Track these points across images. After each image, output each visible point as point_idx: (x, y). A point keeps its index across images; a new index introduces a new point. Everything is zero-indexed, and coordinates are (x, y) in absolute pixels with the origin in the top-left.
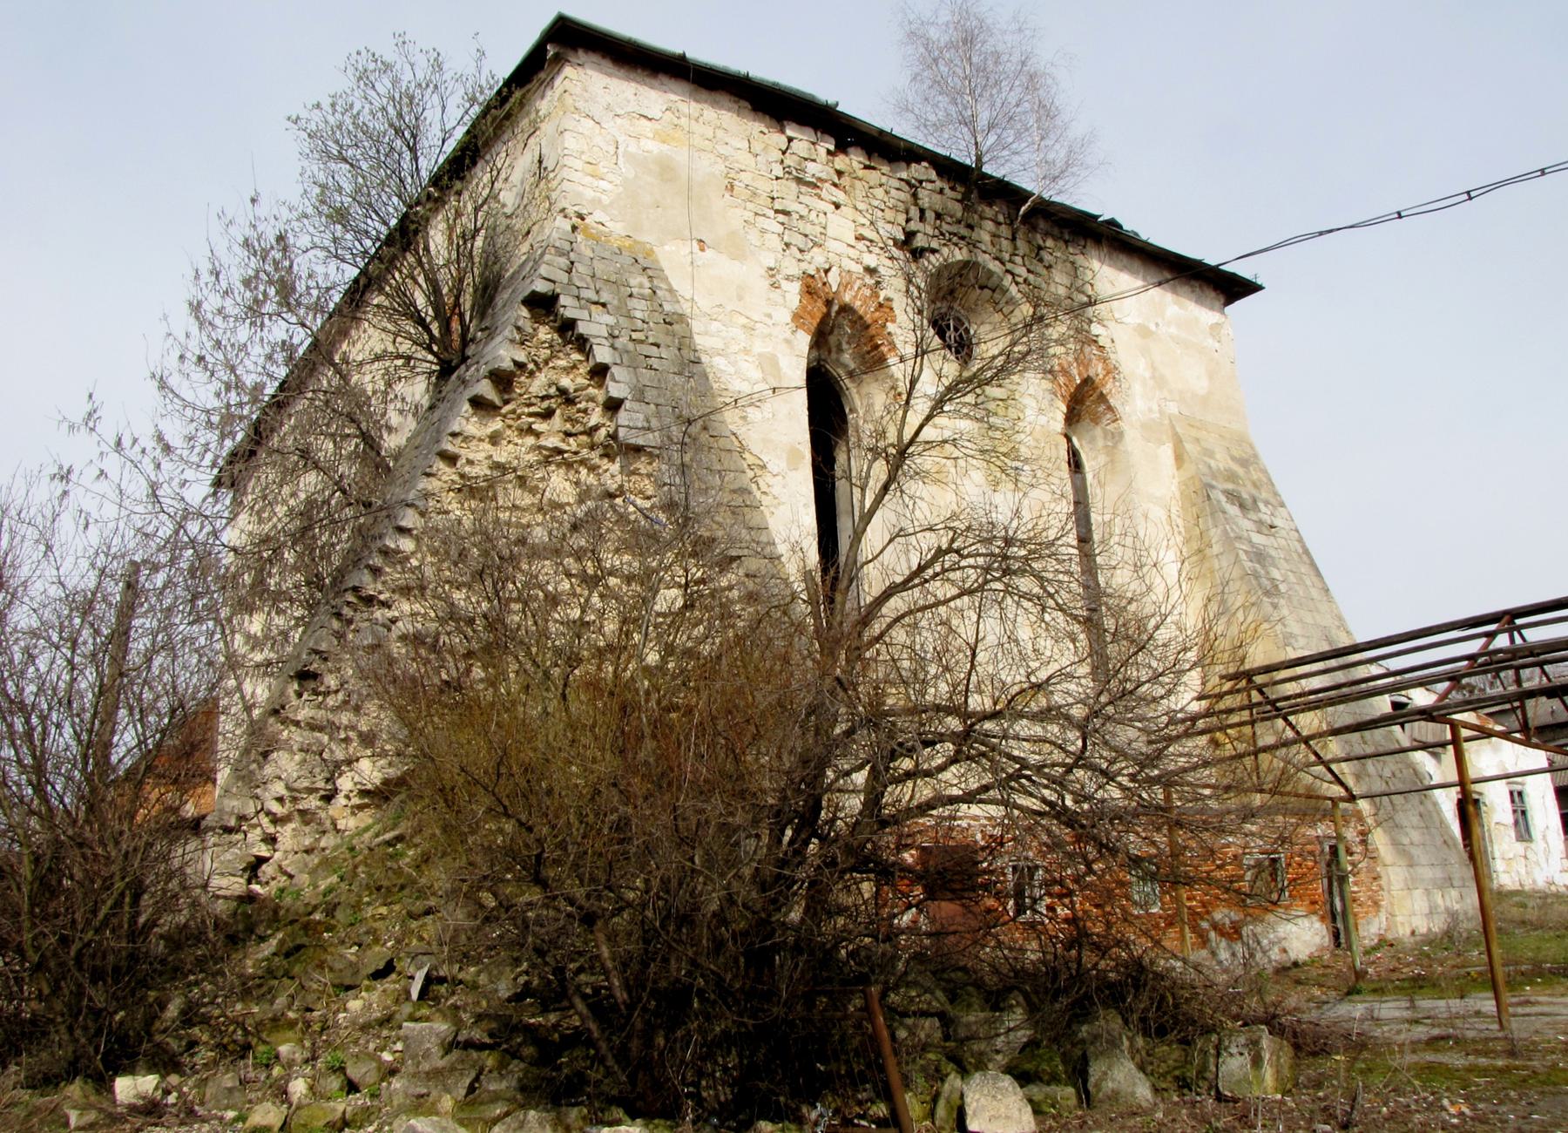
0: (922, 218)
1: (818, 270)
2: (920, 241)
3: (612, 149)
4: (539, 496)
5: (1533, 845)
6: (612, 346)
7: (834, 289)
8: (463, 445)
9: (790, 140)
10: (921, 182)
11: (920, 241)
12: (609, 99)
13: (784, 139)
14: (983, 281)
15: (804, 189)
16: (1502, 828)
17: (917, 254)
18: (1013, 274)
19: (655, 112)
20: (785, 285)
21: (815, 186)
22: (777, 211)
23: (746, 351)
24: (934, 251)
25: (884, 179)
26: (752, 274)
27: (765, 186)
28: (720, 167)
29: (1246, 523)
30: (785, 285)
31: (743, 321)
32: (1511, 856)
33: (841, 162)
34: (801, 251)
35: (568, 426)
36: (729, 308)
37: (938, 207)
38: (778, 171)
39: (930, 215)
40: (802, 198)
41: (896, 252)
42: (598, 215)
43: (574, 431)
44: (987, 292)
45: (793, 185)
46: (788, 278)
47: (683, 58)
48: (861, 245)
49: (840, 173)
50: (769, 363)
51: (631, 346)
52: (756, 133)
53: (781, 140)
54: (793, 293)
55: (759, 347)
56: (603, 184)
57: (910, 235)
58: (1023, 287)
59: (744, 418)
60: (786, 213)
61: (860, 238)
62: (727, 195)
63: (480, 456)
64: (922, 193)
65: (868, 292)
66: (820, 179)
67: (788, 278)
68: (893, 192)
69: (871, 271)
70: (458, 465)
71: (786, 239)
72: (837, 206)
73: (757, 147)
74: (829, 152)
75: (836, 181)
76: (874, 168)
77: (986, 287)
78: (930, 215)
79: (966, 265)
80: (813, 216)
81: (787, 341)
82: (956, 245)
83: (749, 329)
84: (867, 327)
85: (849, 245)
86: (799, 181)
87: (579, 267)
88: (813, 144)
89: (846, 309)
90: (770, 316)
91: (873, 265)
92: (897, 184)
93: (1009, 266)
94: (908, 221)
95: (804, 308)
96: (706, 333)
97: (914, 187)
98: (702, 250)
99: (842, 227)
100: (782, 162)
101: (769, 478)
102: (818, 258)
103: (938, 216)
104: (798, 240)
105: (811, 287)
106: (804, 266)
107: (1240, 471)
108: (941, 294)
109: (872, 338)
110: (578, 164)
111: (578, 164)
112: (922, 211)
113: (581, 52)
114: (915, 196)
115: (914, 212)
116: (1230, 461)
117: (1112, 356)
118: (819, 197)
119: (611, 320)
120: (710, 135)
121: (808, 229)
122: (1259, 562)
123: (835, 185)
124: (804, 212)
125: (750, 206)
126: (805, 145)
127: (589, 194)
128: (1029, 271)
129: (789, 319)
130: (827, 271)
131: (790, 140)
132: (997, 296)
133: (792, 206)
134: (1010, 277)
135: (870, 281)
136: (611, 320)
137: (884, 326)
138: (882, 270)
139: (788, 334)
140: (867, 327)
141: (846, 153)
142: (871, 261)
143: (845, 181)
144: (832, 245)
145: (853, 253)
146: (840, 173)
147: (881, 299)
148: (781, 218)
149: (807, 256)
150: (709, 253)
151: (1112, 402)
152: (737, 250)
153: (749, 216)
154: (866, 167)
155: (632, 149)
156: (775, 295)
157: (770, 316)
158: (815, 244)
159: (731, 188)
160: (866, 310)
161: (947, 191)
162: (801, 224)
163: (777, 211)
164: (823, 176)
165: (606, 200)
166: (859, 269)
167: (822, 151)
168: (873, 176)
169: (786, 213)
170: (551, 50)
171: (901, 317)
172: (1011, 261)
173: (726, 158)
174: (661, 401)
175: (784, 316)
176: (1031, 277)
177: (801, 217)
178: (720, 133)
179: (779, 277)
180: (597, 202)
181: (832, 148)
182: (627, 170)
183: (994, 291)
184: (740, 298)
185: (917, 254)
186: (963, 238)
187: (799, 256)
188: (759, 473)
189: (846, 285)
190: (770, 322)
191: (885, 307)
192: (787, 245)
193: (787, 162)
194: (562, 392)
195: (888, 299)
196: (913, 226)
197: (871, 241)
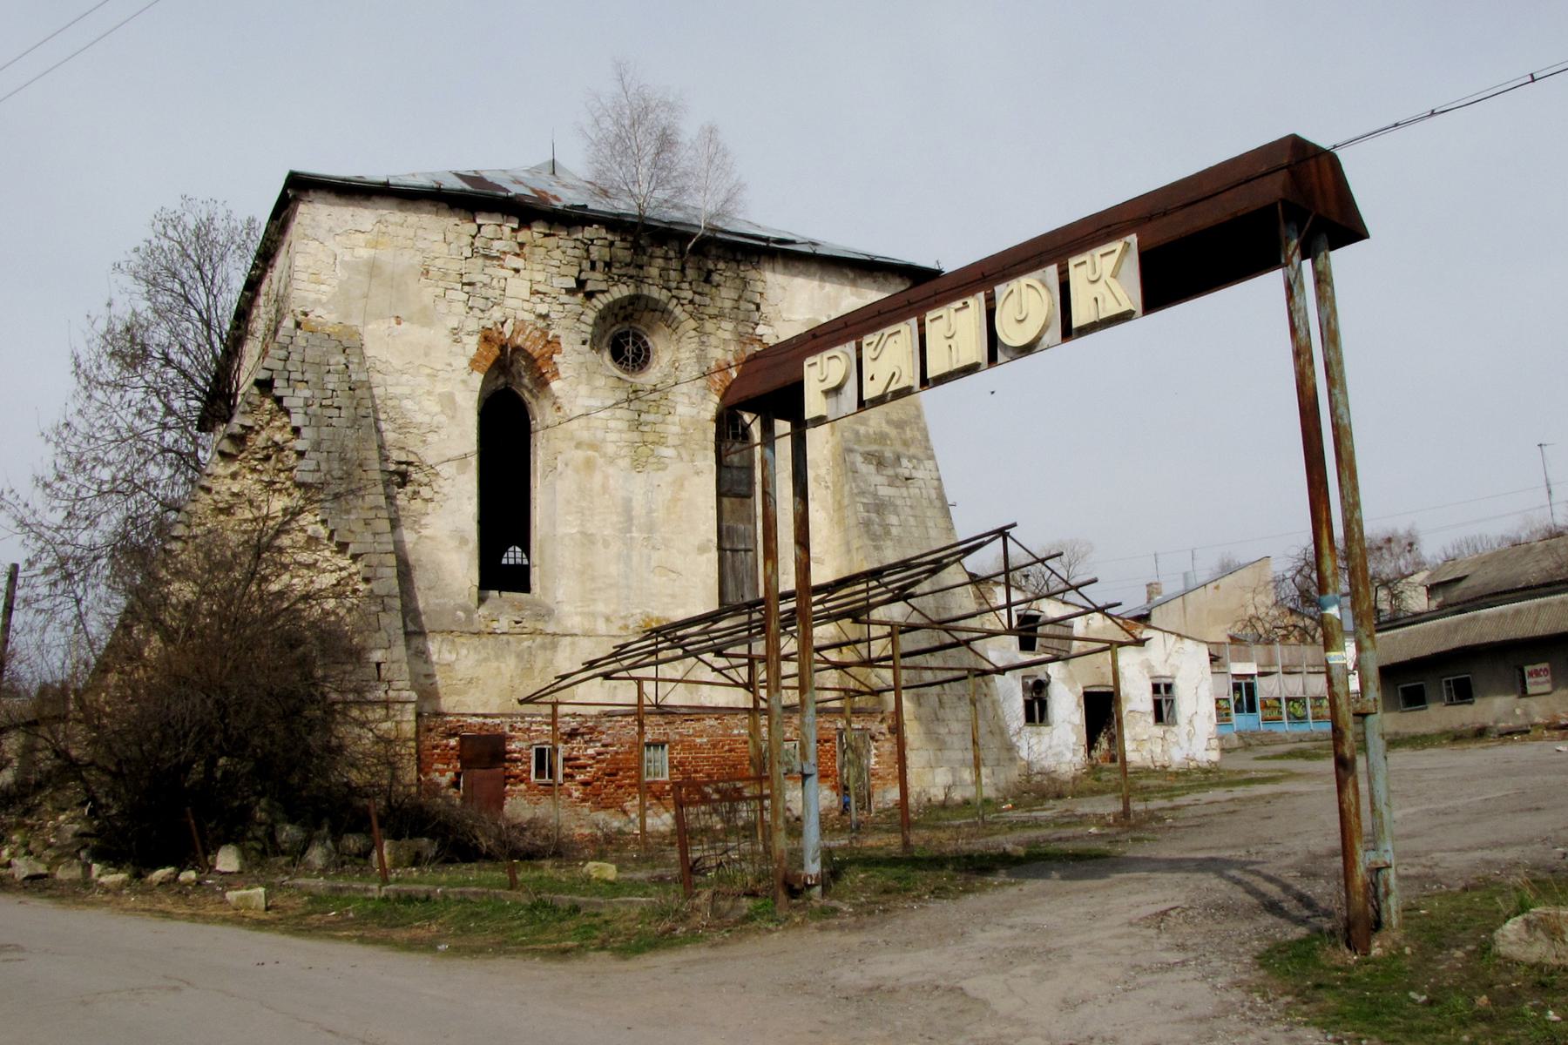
0: (593, 267)
1: (495, 324)
2: (590, 287)
3: (332, 261)
5: (1175, 729)
6: (306, 413)
9: (480, 226)
10: (592, 240)
11: (590, 287)
12: (332, 224)
13: (475, 227)
15: (488, 262)
16: (1138, 715)
18: (678, 299)
19: (368, 227)
20: (466, 339)
21: (498, 258)
22: (464, 284)
23: (429, 393)
24: (603, 292)
25: (561, 242)
26: (438, 336)
27: (455, 266)
28: (419, 258)
29: (879, 479)
30: (466, 339)
31: (429, 371)
32: (1145, 737)
33: (524, 236)
34: (482, 311)
36: (417, 364)
37: (607, 259)
39: (600, 265)
40: (486, 271)
41: (565, 298)
42: (319, 311)
45: (480, 261)
47: (387, 184)
48: (535, 299)
49: (521, 245)
50: (448, 401)
51: (319, 411)
52: (451, 226)
53: (473, 228)
54: (472, 344)
55: (441, 388)
56: (323, 287)
57: (581, 283)
58: (689, 308)
59: (424, 441)
60: (470, 284)
61: (534, 293)
62: (423, 279)
63: (224, 488)
64: (592, 248)
65: (537, 334)
66: (504, 253)
68: (569, 251)
69: (545, 317)
71: (470, 304)
73: (450, 237)
74: (513, 230)
75: (518, 251)
76: (554, 235)
78: (600, 265)
79: (634, 300)
80: (495, 282)
81: (464, 381)
83: (433, 376)
84: (535, 361)
86: (486, 257)
87: (294, 356)
88: (500, 225)
89: (517, 349)
90: (450, 365)
91: (544, 312)
92: (572, 244)
93: (675, 292)
94: (580, 272)
95: (479, 354)
96: (397, 384)
97: (587, 245)
98: (399, 323)
99: (518, 287)
100: (472, 244)
101: (441, 482)
102: (497, 314)
103: (608, 265)
104: (480, 303)
105: (487, 339)
106: (483, 322)
107: (892, 432)
108: (619, 319)
109: (540, 368)
110: (304, 276)
111: (304, 276)
113: (311, 193)
114: (587, 250)
115: (586, 265)
116: (884, 425)
118: (502, 267)
119: (307, 393)
120: (411, 234)
121: (490, 293)
122: (878, 512)
123: (517, 255)
124: (487, 280)
125: (441, 283)
126: (492, 228)
127: (313, 296)
128: (695, 293)
129: (466, 365)
130: (503, 324)
131: (480, 226)
132: (666, 316)
133: (476, 277)
134: (675, 301)
135: (541, 324)
136: (307, 393)
137: (551, 358)
138: (552, 315)
139: (465, 376)
140: (535, 361)
141: (529, 228)
142: (542, 309)
143: (526, 250)
144: (509, 302)
145: (527, 306)
146: (521, 245)
147: (550, 338)
148: (467, 288)
149: (487, 315)
150: (404, 325)
152: (426, 318)
153: (440, 291)
154: (546, 235)
155: (347, 258)
156: (457, 348)
157: (450, 365)
158: (495, 304)
160: (536, 349)
161: (618, 244)
162: (484, 292)
163: (464, 284)
164: (506, 249)
165: (324, 298)
166: (530, 317)
167: (507, 230)
168: (552, 241)
169: (470, 284)
172: (677, 288)
173: (423, 251)
174: (333, 449)
175: (464, 362)
176: (697, 298)
177: (485, 285)
178: (420, 232)
179: (461, 334)
180: (318, 302)
181: (516, 226)
182: (341, 273)
184: (426, 355)
185: (590, 295)
186: (631, 277)
187: (481, 315)
188: (433, 478)
189: (516, 331)
190: (450, 369)
191: (553, 345)
192: (471, 308)
193: (476, 244)
194: (276, 444)
195: (557, 337)
196: (583, 276)
197: (544, 294)
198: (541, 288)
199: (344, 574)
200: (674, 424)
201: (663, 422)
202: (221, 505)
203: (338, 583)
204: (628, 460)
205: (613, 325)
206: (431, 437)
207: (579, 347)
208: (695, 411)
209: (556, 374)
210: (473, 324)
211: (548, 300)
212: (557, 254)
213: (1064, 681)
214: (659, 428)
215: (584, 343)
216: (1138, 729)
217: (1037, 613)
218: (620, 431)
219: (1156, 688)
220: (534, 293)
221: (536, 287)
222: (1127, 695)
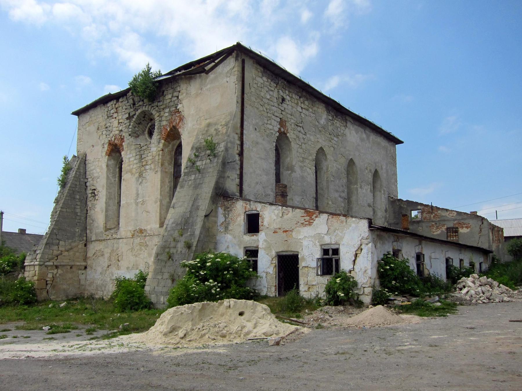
26: (100, 148)
27: (104, 123)
32: (314, 283)
34: (109, 135)
48: (119, 125)
54: (106, 146)
59: (97, 182)
105: (110, 144)
117: (182, 113)
130: (112, 137)
137: (122, 144)
144: (114, 129)
145: (117, 129)
151: (180, 130)
175: (104, 154)
191: (122, 140)
200: (150, 156)
201: (147, 156)
204: (138, 173)
205: (148, 124)
206: (98, 180)
208: (156, 148)
209: (123, 150)
210: (107, 141)
211: (122, 124)
212: (124, 107)
213: (265, 249)
214: (146, 159)
215: (130, 135)
216: (310, 278)
217: (256, 212)
218: (137, 164)
219: (326, 252)
220: (119, 123)
222: (303, 257)
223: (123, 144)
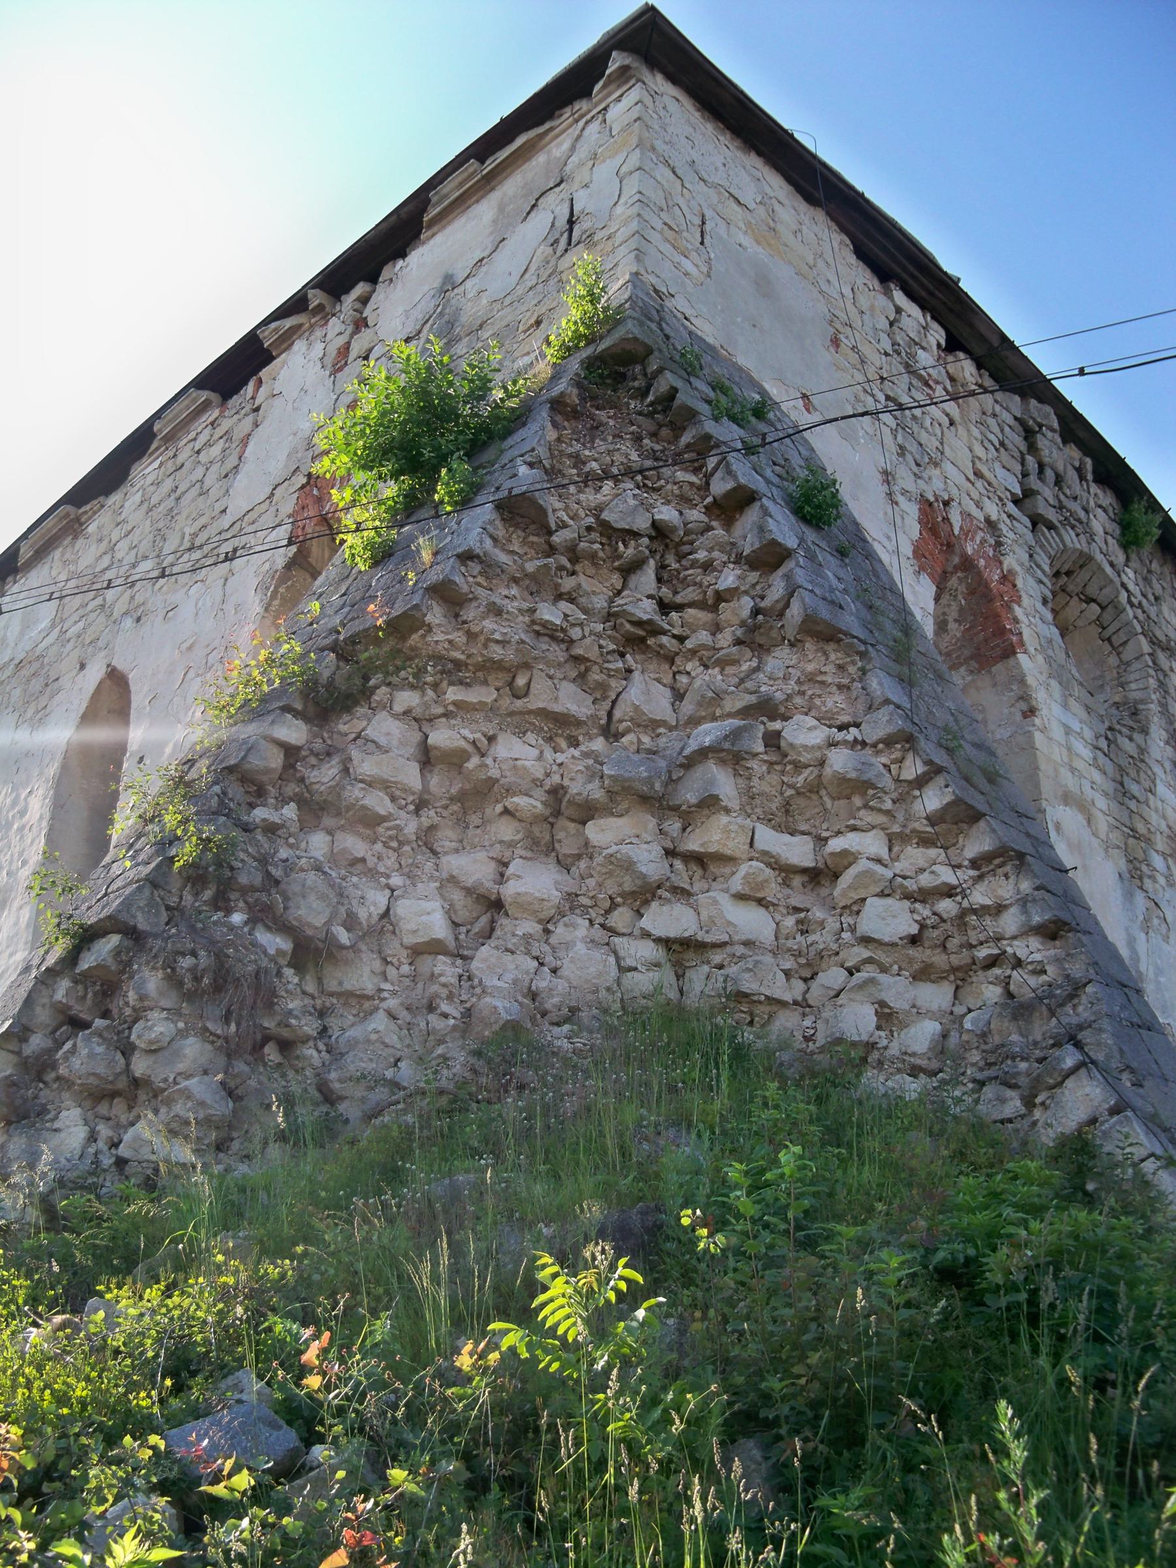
3: (698, 221)
4: (607, 705)
7: (956, 532)
8: (480, 579)
10: (1040, 426)
12: (694, 155)
14: (1092, 590)
17: (1036, 521)
19: (749, 196)
28: (822, 307)
35: (665, 591)
38: (886, 345)
39: (1049, 474)
43: (679, 599)
44: (1094, 607)
46: (904, 492)
57: (1028, 493)
62: (832, 349)
67: (904, 492)
69: (991, 524)
70: (470, 613)
72: (952, 423)
77: (1094, 601)
82: (1073, 527)
85: (968, 479)
91: (994, 517)
92: (1012, 422)
112: (1041, 467)
113: (659, 78)
132: (1107, 616)
138: (1002, 526)
142: (993, 510)
159: (836, 342)
170: (617, 60)
171: (1026, 601)
183: (1103, 608)
189: (967, 533)
198: (984, 470)
199: (947, 906)
202: (497, 652)
203: (914, 940)
207: (1039, 606)
209: (1022, 643)
221: (979, 465)
223: (1018, 611)
